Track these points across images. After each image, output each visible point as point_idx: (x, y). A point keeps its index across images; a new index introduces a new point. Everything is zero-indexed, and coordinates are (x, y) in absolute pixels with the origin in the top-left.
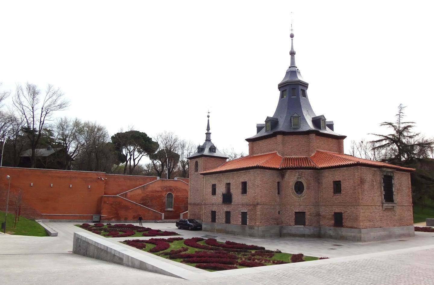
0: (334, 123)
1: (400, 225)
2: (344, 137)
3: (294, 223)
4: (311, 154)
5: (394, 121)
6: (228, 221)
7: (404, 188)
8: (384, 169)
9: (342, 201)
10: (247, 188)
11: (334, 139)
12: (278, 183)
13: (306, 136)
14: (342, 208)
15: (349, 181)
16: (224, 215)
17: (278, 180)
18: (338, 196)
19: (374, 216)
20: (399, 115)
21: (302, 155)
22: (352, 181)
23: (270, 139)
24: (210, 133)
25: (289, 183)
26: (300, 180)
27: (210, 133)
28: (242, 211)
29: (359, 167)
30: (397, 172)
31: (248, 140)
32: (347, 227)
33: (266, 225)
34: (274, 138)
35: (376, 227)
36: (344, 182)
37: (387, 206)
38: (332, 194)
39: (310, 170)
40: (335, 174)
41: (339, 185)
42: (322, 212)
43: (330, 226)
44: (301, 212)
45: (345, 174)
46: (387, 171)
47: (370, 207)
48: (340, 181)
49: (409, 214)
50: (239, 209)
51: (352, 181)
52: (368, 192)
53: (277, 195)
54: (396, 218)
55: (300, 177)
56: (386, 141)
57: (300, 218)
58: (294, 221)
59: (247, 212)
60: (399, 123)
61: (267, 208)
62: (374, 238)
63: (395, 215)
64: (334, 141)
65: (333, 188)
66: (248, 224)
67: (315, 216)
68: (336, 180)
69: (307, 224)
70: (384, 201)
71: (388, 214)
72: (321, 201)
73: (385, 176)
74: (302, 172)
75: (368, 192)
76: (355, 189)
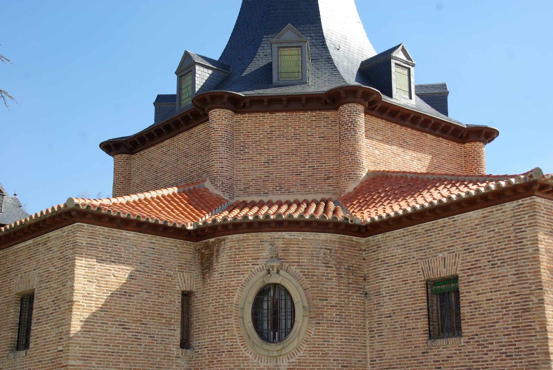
0: (449, 89)
2: (487, 134)
4: (346, 187)
10: (34, 321)
11: (445, 141)
12: (186, 296)
13: (328, 113)
15: (497, 271)
17: (186, 280)
18: (446, 346)
21: (308, 193)
22: (509, 270)
23: (186, 134)
25: (230, 293)
26: (275, 279)
29: (539, 200)
31: (111, 147)
34: (201, 127)
36: (472, 278)
39: (323, 236)
40: (431, 245)
41: (453, 295)
48: (455, 279)
53: (176, 350)
55: (276, 264)
64: (447, 146)
65: (425, 312)
68: (437, 276)
74: (288, 243)
76: (528, 310)
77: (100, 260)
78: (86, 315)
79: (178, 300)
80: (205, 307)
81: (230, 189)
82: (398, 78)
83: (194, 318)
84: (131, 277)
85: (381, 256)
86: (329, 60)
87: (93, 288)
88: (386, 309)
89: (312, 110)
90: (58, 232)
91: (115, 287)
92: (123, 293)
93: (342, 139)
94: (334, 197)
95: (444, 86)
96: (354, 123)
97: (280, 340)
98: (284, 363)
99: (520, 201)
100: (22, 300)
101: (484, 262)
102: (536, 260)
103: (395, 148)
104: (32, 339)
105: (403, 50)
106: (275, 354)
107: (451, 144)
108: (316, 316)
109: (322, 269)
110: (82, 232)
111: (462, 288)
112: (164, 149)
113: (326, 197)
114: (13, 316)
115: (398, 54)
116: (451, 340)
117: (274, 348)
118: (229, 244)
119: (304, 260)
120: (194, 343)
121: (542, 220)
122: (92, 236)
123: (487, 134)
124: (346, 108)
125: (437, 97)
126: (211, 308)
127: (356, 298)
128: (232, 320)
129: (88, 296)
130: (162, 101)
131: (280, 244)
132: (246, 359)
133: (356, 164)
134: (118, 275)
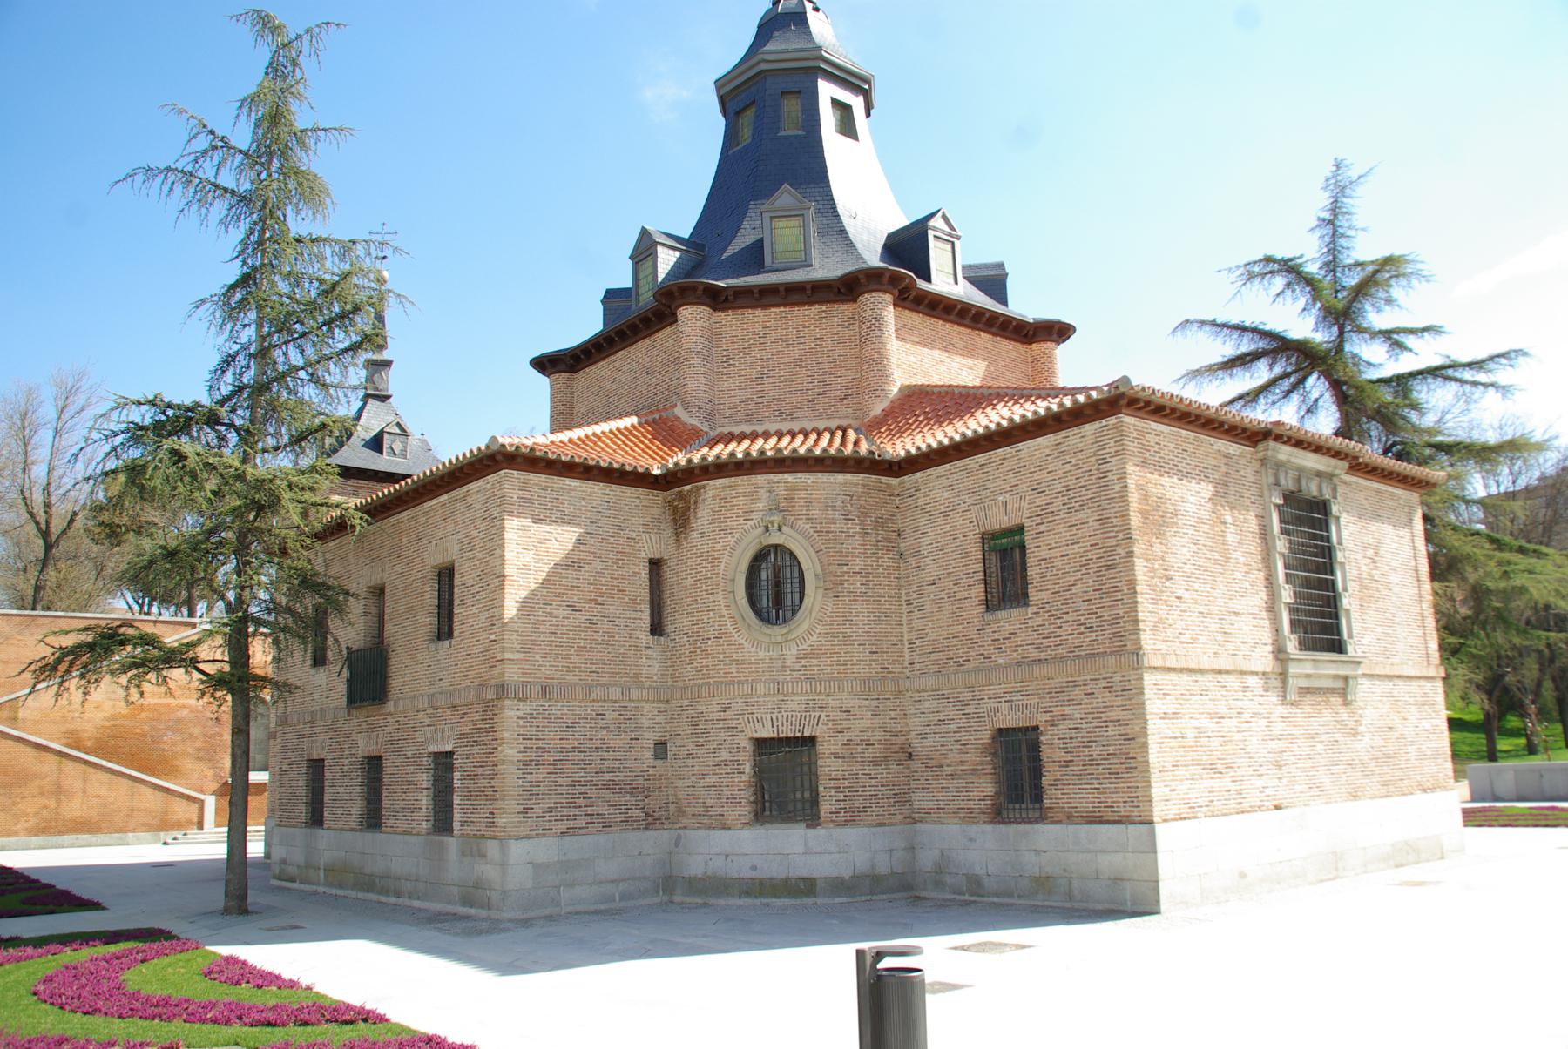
1: (1391, 788)
2: (1059, 331)
3: (745, 811)
5: (1311, 257)
6: (373, 819)
7: (1394, 578)
8: (1284, 452)
9: (1033, 654)
10: (456, 602)
12: (656, 565)
13: (843, 307)
14: (1034, 700)
15: (1075, 517)
16: (357, 777)
17: (655, 544)
18: (1009, 620)
19: (1238, 736)
20: (1333, 224)
21: (819, 418)
22: (1088, 515)
23: (647, 341)
24: (387, 364)
25: (714, 559)
26: (776, 539)
27: (387, 364)
28: (433, 748)
29: (1127, 419)
30: (1355, 479)
31: (545, 364)
32: (1070, 819)
33: (562, 826)
34: (668, 331)
35: (1252, 810)
36: (1042, 528)
37: (1308, 676)
38: (974, 609)
39: (840, 477)
40: (988, 485)
42: (923, 735)
43: (970, 818)
44: (787, 738)
45: (1050, 477)
46: (1301, 470)
47: (1206, 681)
48: (1020, 529)
49: (1428, 726)
50: (417, 735)
51: (1088, 515)
52: (1196, 586)
53: (644, 637)
54: (1362, 746)
55: (777, 518)
56: (1271, 367)
57: (784, 777)
58: (748, 795)
59: (451, 754)
60: (1332, 265)
61: (570, 717)
62: (1243, 875)
63: (1355, 733)
64: (1008, 348)
66: (456, 825)
67: (875, 761)
68: (996, 527)
69: (825, 808)
70: (1292, 645)
71: (1314, 723)
72: (918, 666)
73: (1288, 497)
74: (792, 489)
75: (1196, 586)
76: (1111, 567)
77: (537, 520)
78: (524, 594)
79: (644, 571)
80: (679, 579)
81: (710, 416)
82: (938, 256)
83: (667, 595)
84: (579, 542)
85: (920, 502)
86: (842, 232)
87: (529, 557)
88: (927, 575)
89: (821, 303)
90: (479, 484)
91: (560, 556)
92: (570, 563)
93: (863, 341)
94: (855, 423)
95: (1001, 266)
96: (879, 319)
97: (785, 621)
98: (791, 652)
99: (1104, 422)
100: (439, 575)
101: (1057, 505)
102: (1124, 500)
103: (937, 353)
104: (456, 626)
105: (944, 217)
106: (779, 639)
107: (1013, 345)
108: (833, 587)
109: (840, 523)
110: (511, 481)
111: (1029, 542)
112: (618, 364)
113: (844, 423)
114: (430, 597)
115: (937, 222)
116: (1015, 611)
117: (778, 631)
118: (711, 493)
119: (816, 511)
120: (669, 628)
121: (1131, 446)
122: (525, 487)
123: (1059, 331)
124: (868, 299)
125: (993, 281)
126: (690, 581)
127: (887, 560)
128: (719, 596)
129: (524, 568)
130: (611, 296)
131: (781, 490)
132: (741, 647)
133: (883, 376)
134: (562, 539)
